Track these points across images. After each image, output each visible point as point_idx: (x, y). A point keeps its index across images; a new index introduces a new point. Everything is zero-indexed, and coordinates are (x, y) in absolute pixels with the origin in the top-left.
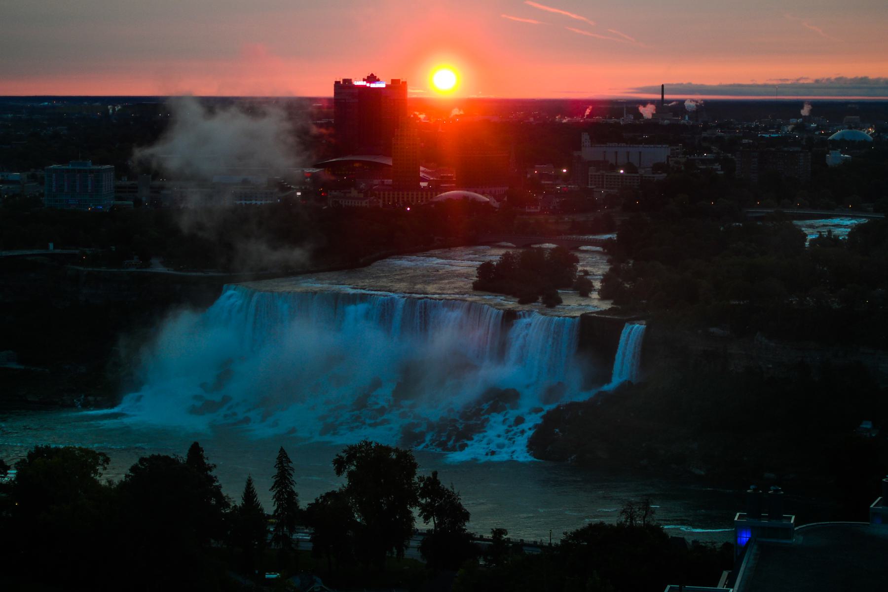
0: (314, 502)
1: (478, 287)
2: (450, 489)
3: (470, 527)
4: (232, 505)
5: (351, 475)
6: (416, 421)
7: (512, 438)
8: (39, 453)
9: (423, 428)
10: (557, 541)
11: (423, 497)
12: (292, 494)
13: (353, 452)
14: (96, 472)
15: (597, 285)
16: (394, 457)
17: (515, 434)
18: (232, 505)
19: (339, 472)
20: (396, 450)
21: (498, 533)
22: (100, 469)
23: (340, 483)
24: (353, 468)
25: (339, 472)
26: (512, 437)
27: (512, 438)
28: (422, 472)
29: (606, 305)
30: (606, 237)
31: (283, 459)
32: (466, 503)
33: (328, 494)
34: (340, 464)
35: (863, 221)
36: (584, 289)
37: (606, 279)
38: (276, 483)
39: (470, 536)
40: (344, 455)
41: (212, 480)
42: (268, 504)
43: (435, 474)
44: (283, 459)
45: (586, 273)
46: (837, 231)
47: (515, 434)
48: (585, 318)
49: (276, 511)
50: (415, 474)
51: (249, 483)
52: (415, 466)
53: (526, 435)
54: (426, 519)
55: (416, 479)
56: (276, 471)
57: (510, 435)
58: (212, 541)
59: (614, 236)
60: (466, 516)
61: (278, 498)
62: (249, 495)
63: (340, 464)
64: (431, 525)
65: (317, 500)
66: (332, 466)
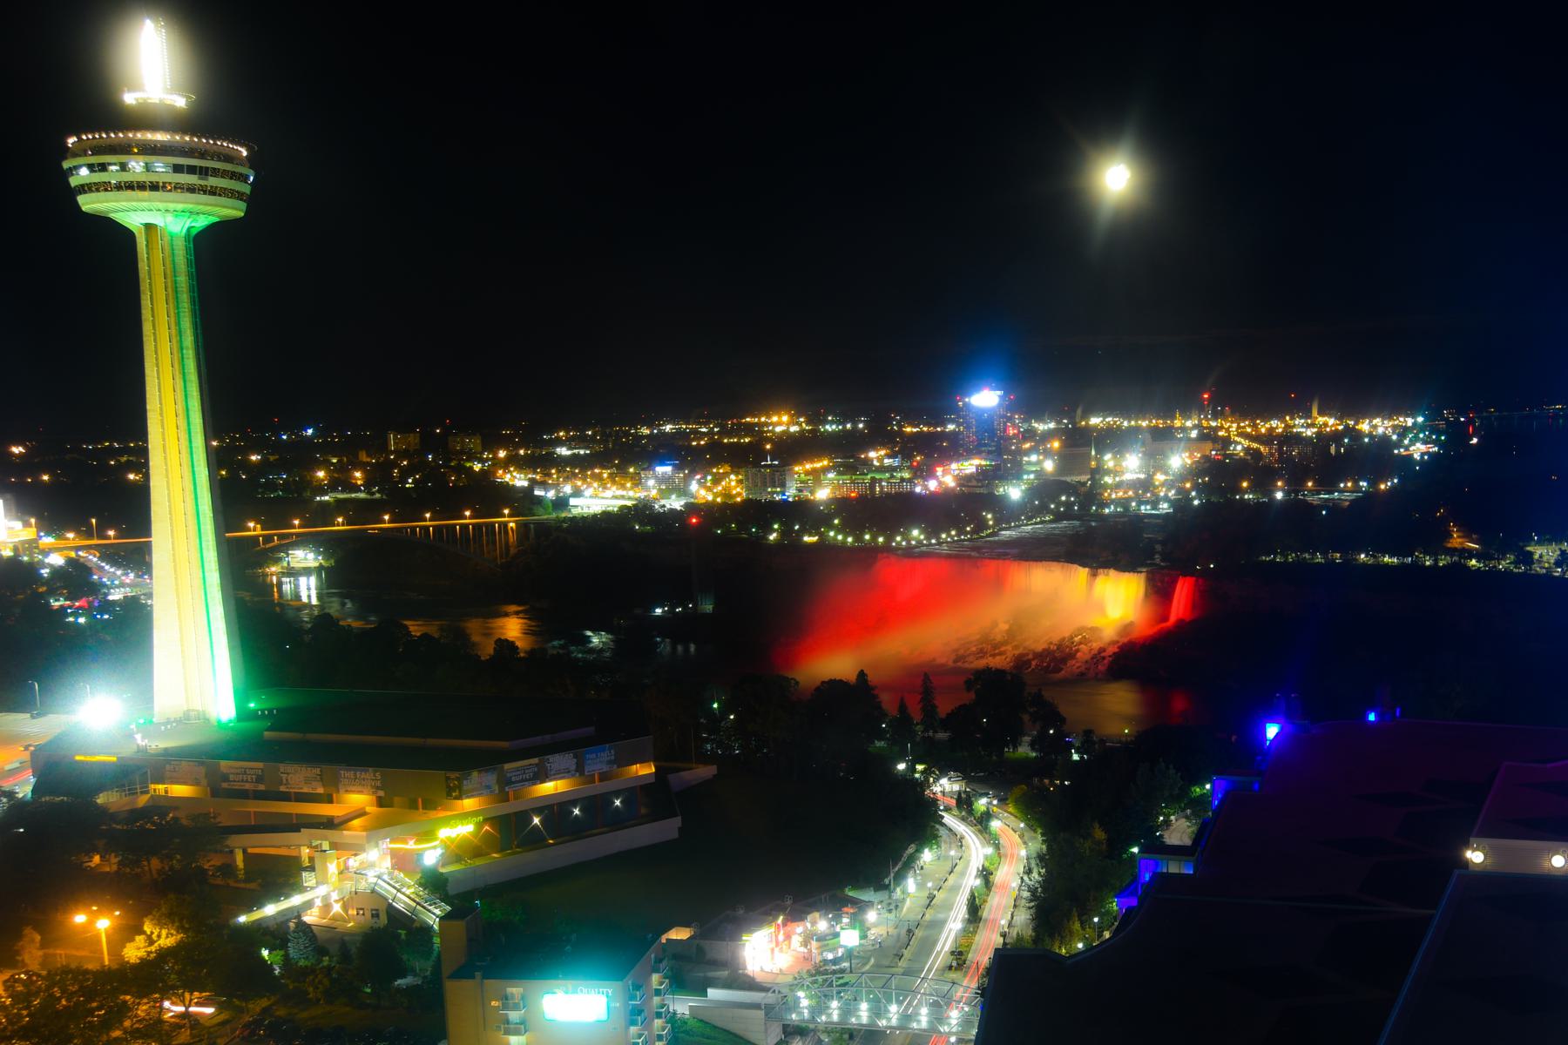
0: (950, 711)
2: (1051, 701)
6: (1024, 652)
9: (1031, 656)
16: (1010, 678)
19: (969, 690)
23: (969, 697)
24: (979, 686)
25: (969, 690)
33: (960, 706)
38: (922, 698)
40: (972, 677)
53: (1106, 661)
58: (876, 742)
62: (903, 708)
63: (969, 685)
65: (952, 710)
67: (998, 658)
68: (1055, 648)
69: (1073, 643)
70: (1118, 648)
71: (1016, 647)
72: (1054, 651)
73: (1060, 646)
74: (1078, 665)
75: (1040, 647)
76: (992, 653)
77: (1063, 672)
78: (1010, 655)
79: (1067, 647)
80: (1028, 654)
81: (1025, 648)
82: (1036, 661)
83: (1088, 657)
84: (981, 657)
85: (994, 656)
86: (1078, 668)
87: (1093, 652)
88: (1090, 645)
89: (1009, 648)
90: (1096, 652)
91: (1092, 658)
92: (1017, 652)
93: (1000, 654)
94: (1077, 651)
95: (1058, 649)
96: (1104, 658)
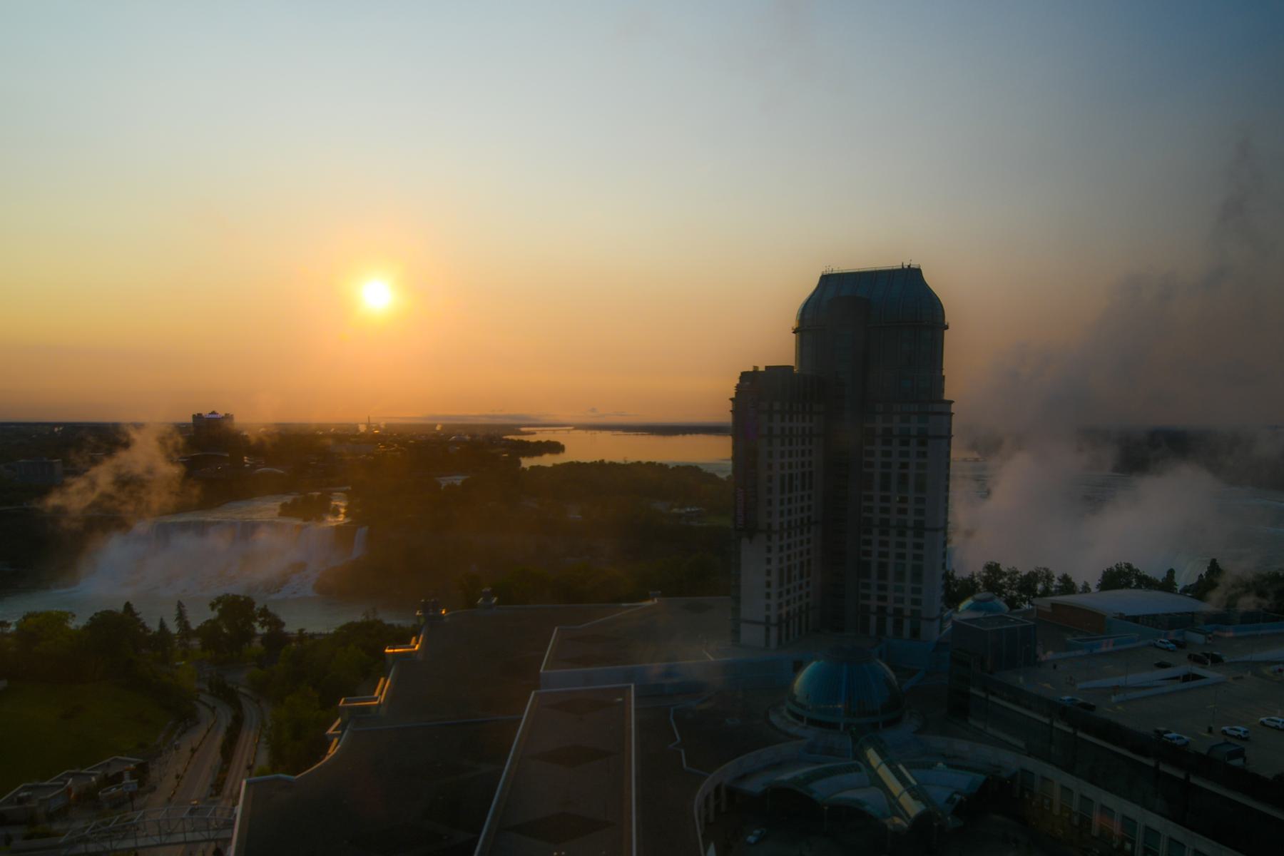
1: (280, 515)
3: (287, 629)
4: (153, 631)
5: (219, 610)
8: (30, 615)
10: (332, 631)
11: (260, 617)
12: (186, 623)
13: (219, 600)
14: (67, 622)
15: (343, 510)
18: (153, 631)
20: (244, 597)
21: (301, 631)
22: (70, 621)
23: (214, 615)
28: (259, 605)
29: (347, 520)
30: (345, 488)
31: (180, 605)
32: (283, 618)
33: (208, 621)
34: (213, 606)
35: (468, 477)
36: (336, 513)
37: (346, 508)
39: (286, 634)
41: (139, 620)
42: (173, 628)
43: (266, 606)
44: (180, 605)
45: (336, 505)
46: (455, 482)
48: (337, 526)
49: (179, 631)
50: (254, 607)
51: (162, 619)
52: (254, 603)
54: (263, 627)
55: (255, 609)
56: (177, 612)
59: (350, 488)
60: (283, 624)
61: (179, 625)
62: (162, 625)
63: (213, 606)
64: (265, 630)
66: (209, 608)
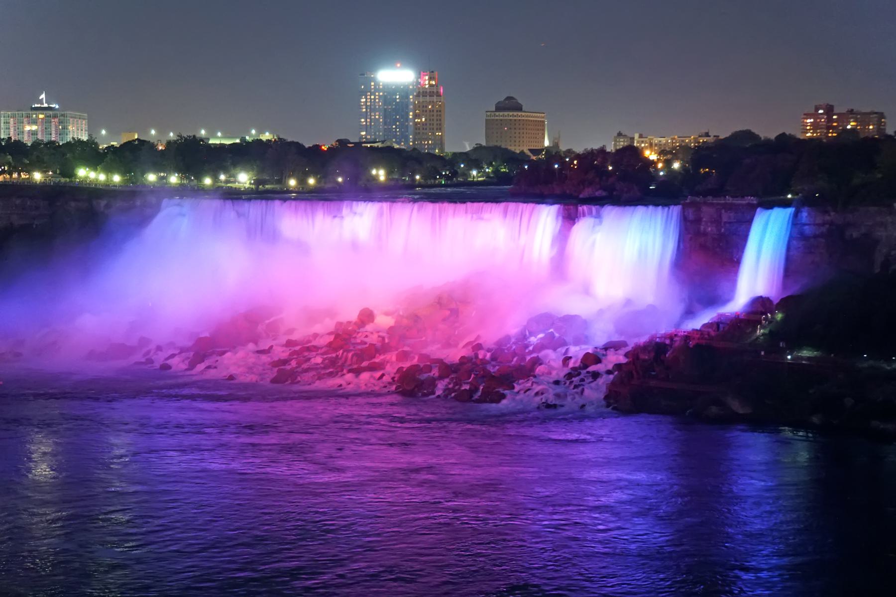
7: (580, 385)
9: (435, 372)
17: (582, 380)
26: (577, 384)
27: (580, 385)
47: (582, 380)
53: (600, 381)
57: (576, 380)
67: (365, 376)
68: (489, 355)
69: (527, 346)
70: (626, 355)
71: (404, 356)
72: (484, 362)
73: (498, 353)
74: (537, 388)
75: (454, 355)
76: (355, 366)
77: (504, 402)
78: (391, 370)
79: (514, 354)
80: (429, 369)
81: (423, 357)
82: (447, 380)
83: (559, 373)
84: (331, 375)
85: (357, 372)
86: (537, 394)
87: (571, 364)
88: (563, 350)
89: (392, 356)
90: (577, 365)
91: (569, 376)
92: (406, 365)
93: (372, 368)
94: (537, 362)
95: (494, 358)
96: (596, 375)
